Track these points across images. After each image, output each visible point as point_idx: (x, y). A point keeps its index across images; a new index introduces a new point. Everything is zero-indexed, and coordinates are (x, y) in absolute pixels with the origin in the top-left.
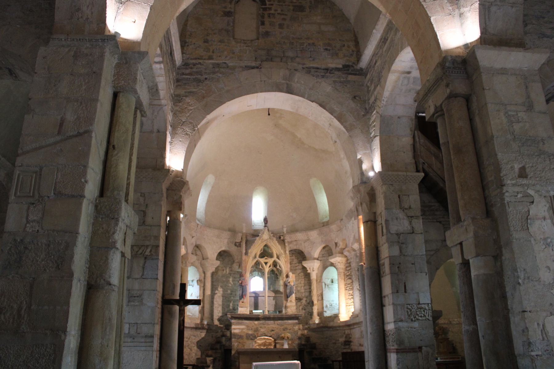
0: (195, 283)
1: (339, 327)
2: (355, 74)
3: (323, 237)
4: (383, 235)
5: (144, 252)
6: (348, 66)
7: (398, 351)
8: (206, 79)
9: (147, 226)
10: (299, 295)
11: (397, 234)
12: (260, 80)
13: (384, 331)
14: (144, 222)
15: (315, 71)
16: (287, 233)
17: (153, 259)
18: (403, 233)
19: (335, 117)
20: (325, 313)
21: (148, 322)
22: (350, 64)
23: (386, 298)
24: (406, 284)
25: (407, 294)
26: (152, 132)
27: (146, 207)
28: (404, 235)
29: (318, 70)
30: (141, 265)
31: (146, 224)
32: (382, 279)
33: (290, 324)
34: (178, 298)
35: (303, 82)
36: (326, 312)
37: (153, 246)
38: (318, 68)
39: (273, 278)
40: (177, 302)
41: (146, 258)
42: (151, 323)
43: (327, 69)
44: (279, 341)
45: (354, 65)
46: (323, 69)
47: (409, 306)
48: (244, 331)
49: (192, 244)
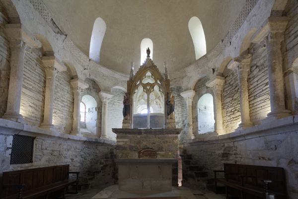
0: (94, 109)
1: (217, 140)
44: (160, 153)
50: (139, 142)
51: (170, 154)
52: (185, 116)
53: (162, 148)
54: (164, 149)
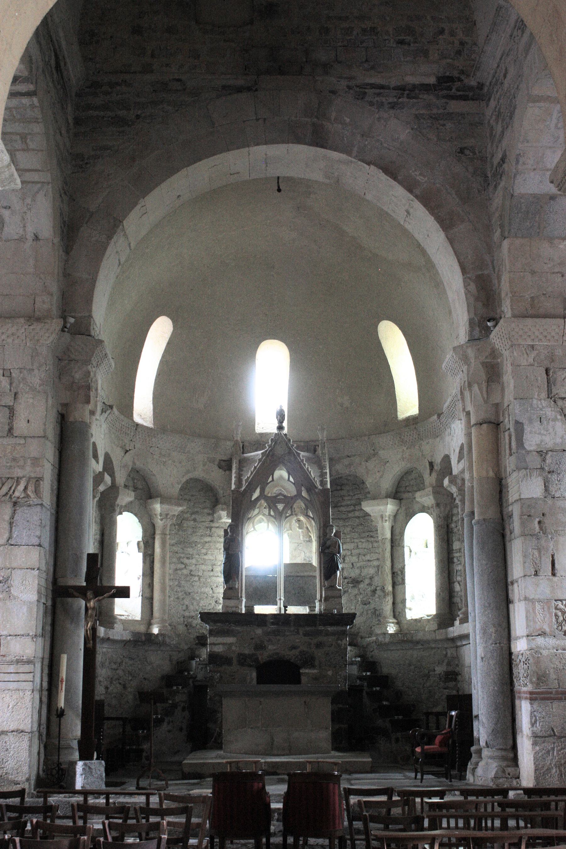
2: (465, 98)
3: (405, 448)
4: (511, 455)
5: (12, 491)
6: (450, 79)
7: (533, 697)
8: (138, 117)
9: (16, 437)
10: (354, 573)
11: (540, 453)
12: (255, 118)
13: (511, 654)
14: (10, 430)
15: (375, 94)
16: (327, 440)
17: (30, 506)
18: (551, 451)
19: (416, 197)
20: (407, 611)
21: (22, 633)
22: (456, 74)
23: (515, 585)
24: (555, 557)
25: (555, 579)
26: (22, 239)
27: (15, 399)
28: (555, 453)
29: (382, 91)
30: (7, 517)
31: (15, 435)
32: (508, 544)
33: (333, 634)
34: (84, 584)
35: (348, 120)
36: (410, 609)
37: (30, 479)
38: (382, 87)
39: (301, 537)
40: (81, 592)
41: (15, 504)
42: (28, 635)
43: (401, 89)
45: (463, 77)
46: (394, 89)
47: (559, 603)
48: (234, 648)
49: (125, 466)
50: (260, 647)
51: (330, 673)
52: (376, 563)
53: (313, 658)
54: (317, 663)
